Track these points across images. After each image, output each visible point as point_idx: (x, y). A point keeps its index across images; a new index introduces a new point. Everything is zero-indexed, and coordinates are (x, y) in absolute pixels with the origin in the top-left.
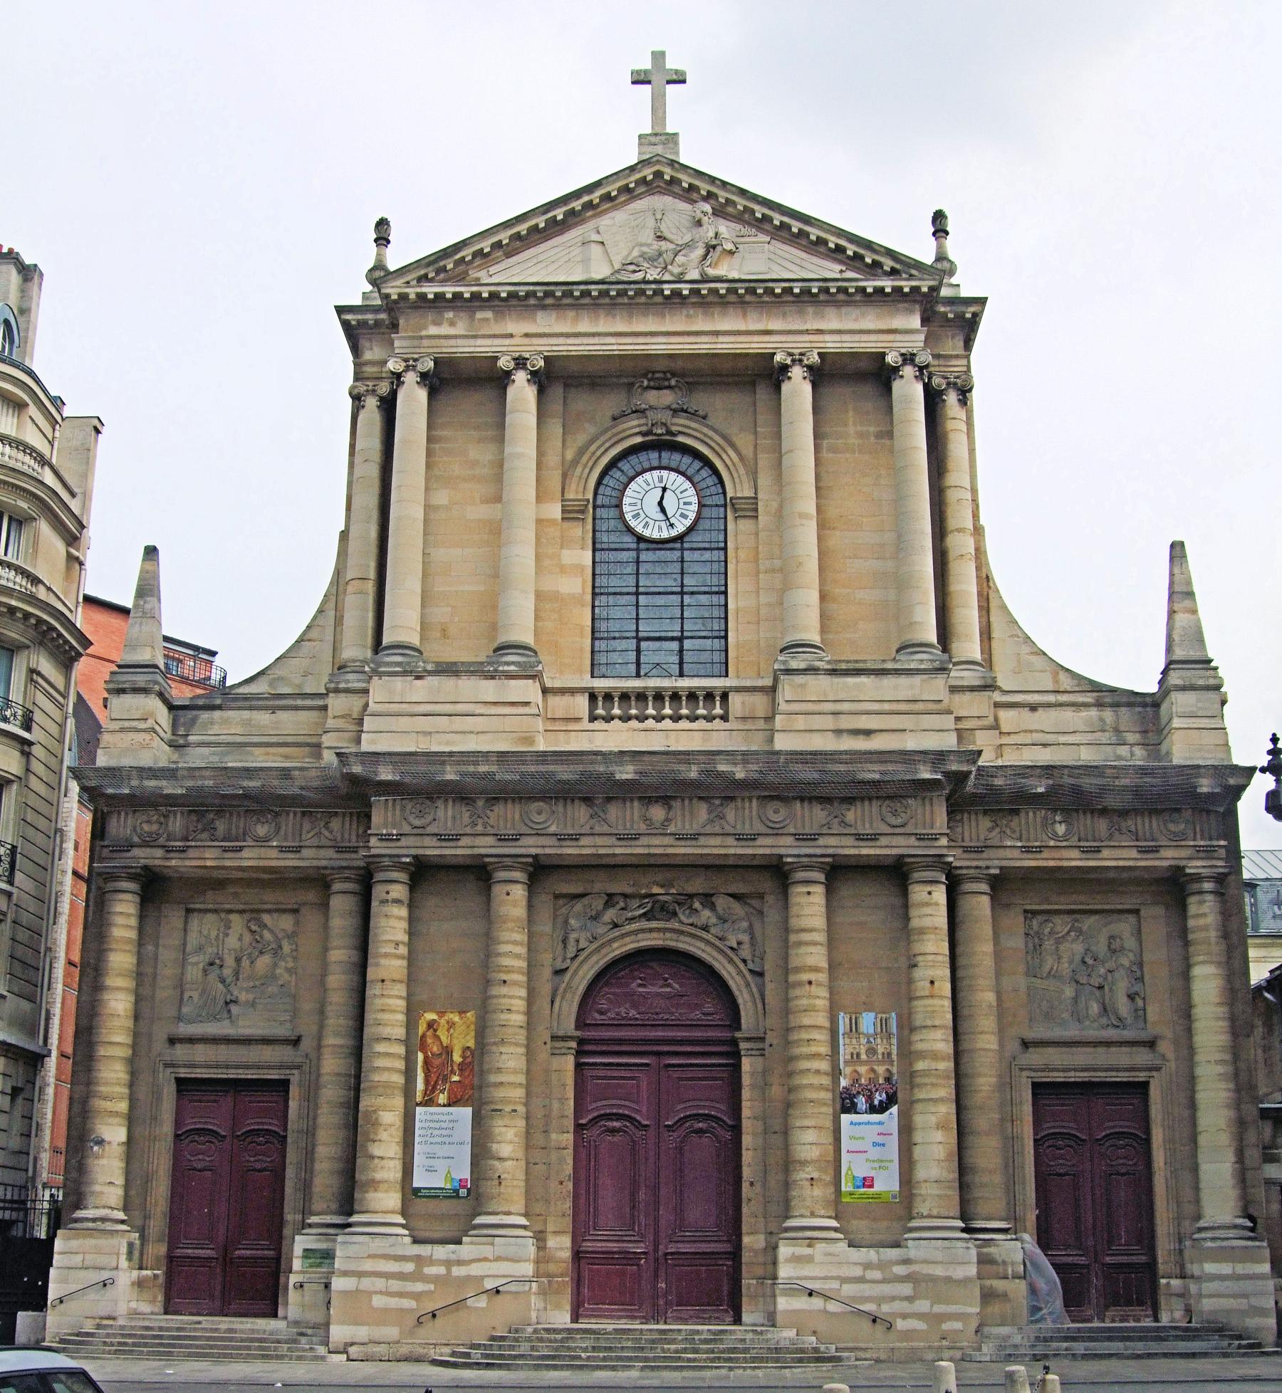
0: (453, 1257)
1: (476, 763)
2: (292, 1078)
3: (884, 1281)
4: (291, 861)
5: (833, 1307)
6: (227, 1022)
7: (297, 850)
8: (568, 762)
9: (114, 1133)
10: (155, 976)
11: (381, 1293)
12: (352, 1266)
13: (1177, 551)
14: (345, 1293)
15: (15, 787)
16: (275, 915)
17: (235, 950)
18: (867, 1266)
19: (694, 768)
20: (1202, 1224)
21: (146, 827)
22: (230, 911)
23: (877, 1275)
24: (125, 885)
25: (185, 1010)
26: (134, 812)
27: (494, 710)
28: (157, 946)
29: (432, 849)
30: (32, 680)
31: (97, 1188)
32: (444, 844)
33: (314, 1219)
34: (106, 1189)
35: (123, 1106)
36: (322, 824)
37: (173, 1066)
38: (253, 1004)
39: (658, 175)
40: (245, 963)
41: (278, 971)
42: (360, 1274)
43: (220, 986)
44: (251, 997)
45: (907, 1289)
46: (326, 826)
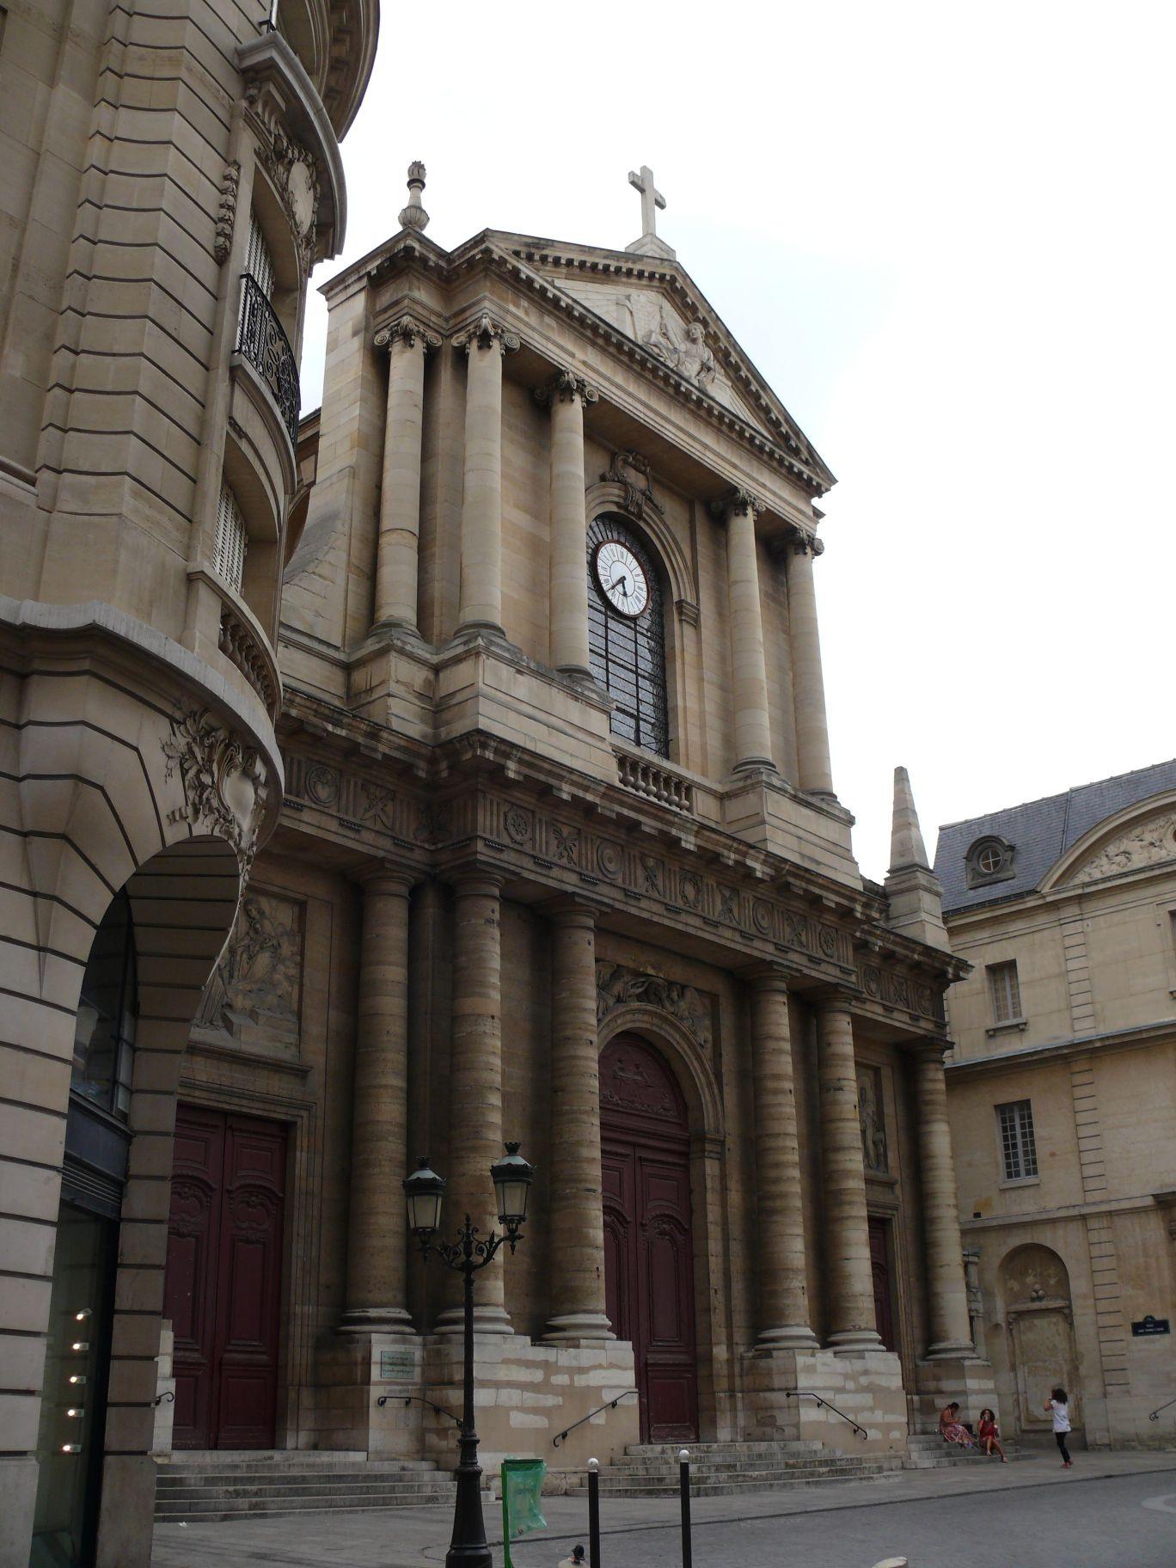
0: (574, 1363)
3: (857, 1391)
5: (834, 1418)
6: (224, 1033)
7: (356, 828)
8: (655, 817)
11: (516, 1408)
13: (901, 775)
16: (274, 903)
18: (846, 1377)
19: (732, 856)
20: (942, 1345)
23: (850, 1385)
27: (580, 735)
39: (673, 279)
41: (278, 977)
44: (248, 1004)
45: (867, 1399)
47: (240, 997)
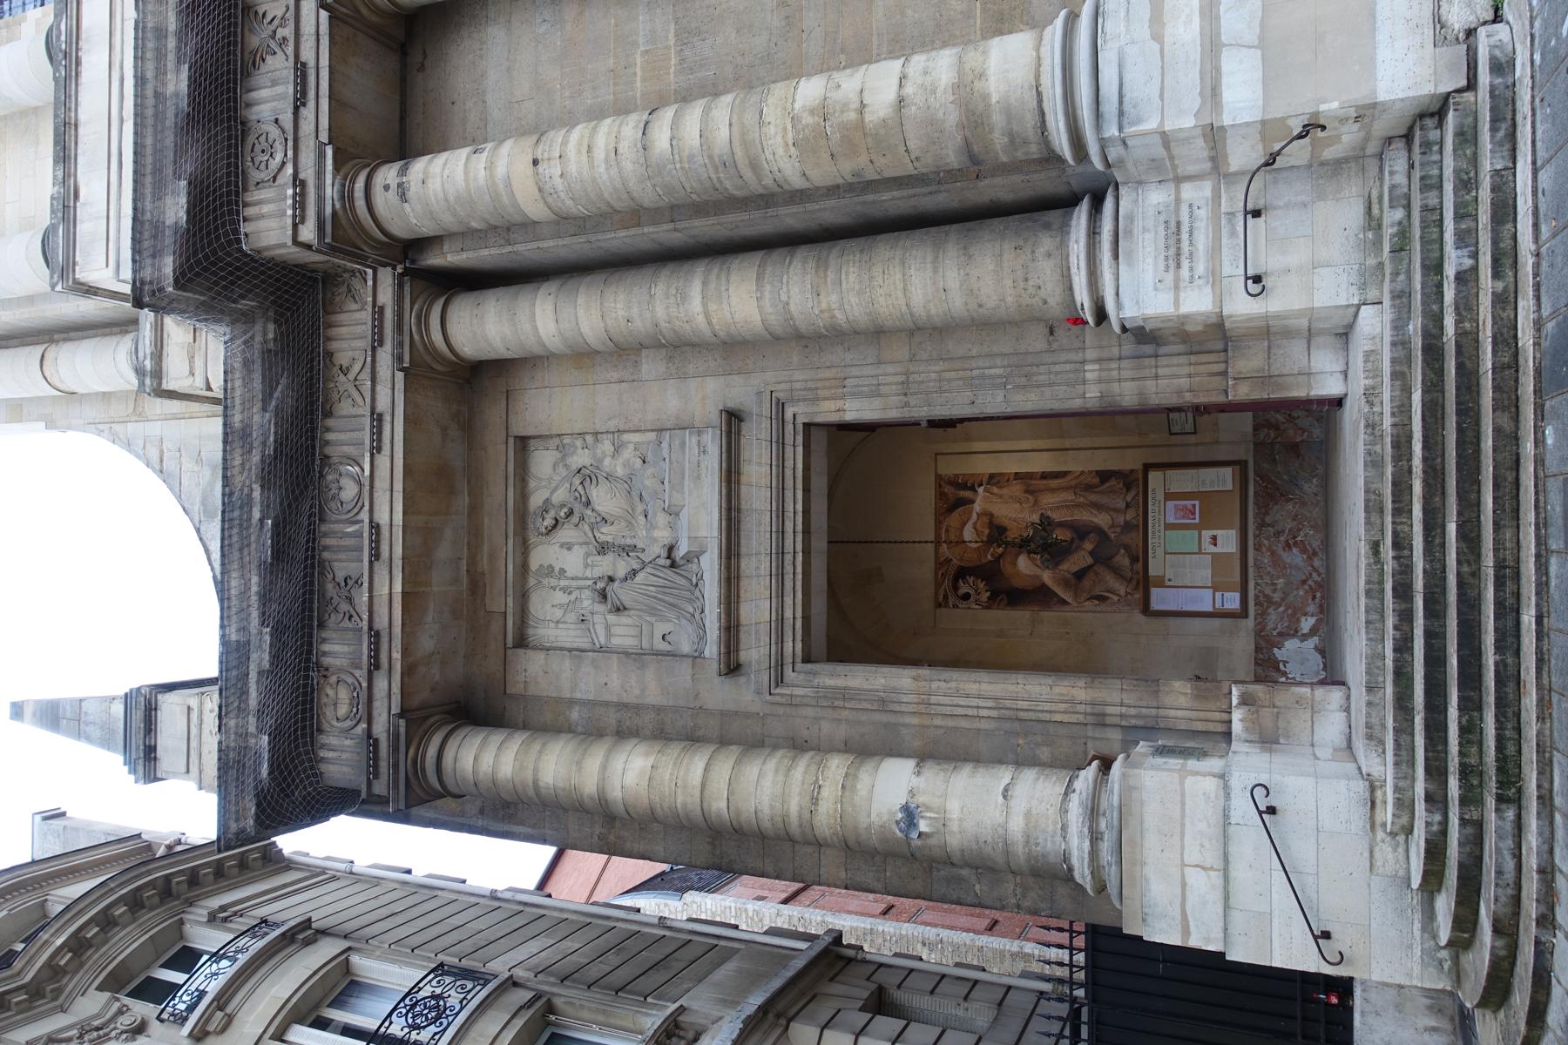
1: (160, 33)
2: (801, 420)
4: (396, 430)
7: (377, 419)
9: (888, 789)
10: (622, 706)
12: (1188, 81)
14: (1268, 82)
15: (355, 959)
16: (532, 484)
17: (588, 555)
21: (343, 710)
22: (523, 569)
24: (432, 751)
25: (686, 648)
26: (320, 730)
28: (572, 702)
29: (317, 118)
30: (225, 920)
31: (1016, 825)
32: (311, 94)
33: (1082, 296)
34: (1020, 802)
35: (837, 766)
36: (342, 378)
37: (781, 665)
38: (673, 512)
40: (607, 534)
41: (620, 471)
42: (1212, 46)
43: (640, 577)
44: (662, 519)
46: (345, 371)
47: (657, 533)
